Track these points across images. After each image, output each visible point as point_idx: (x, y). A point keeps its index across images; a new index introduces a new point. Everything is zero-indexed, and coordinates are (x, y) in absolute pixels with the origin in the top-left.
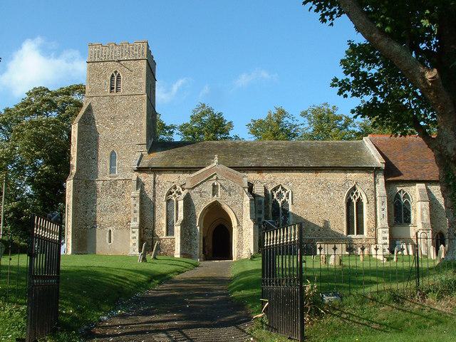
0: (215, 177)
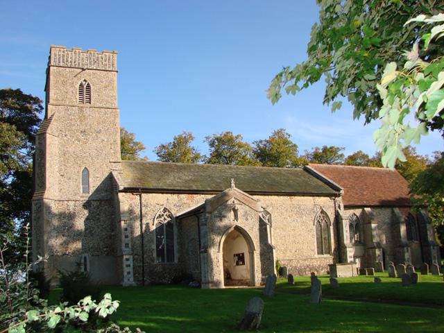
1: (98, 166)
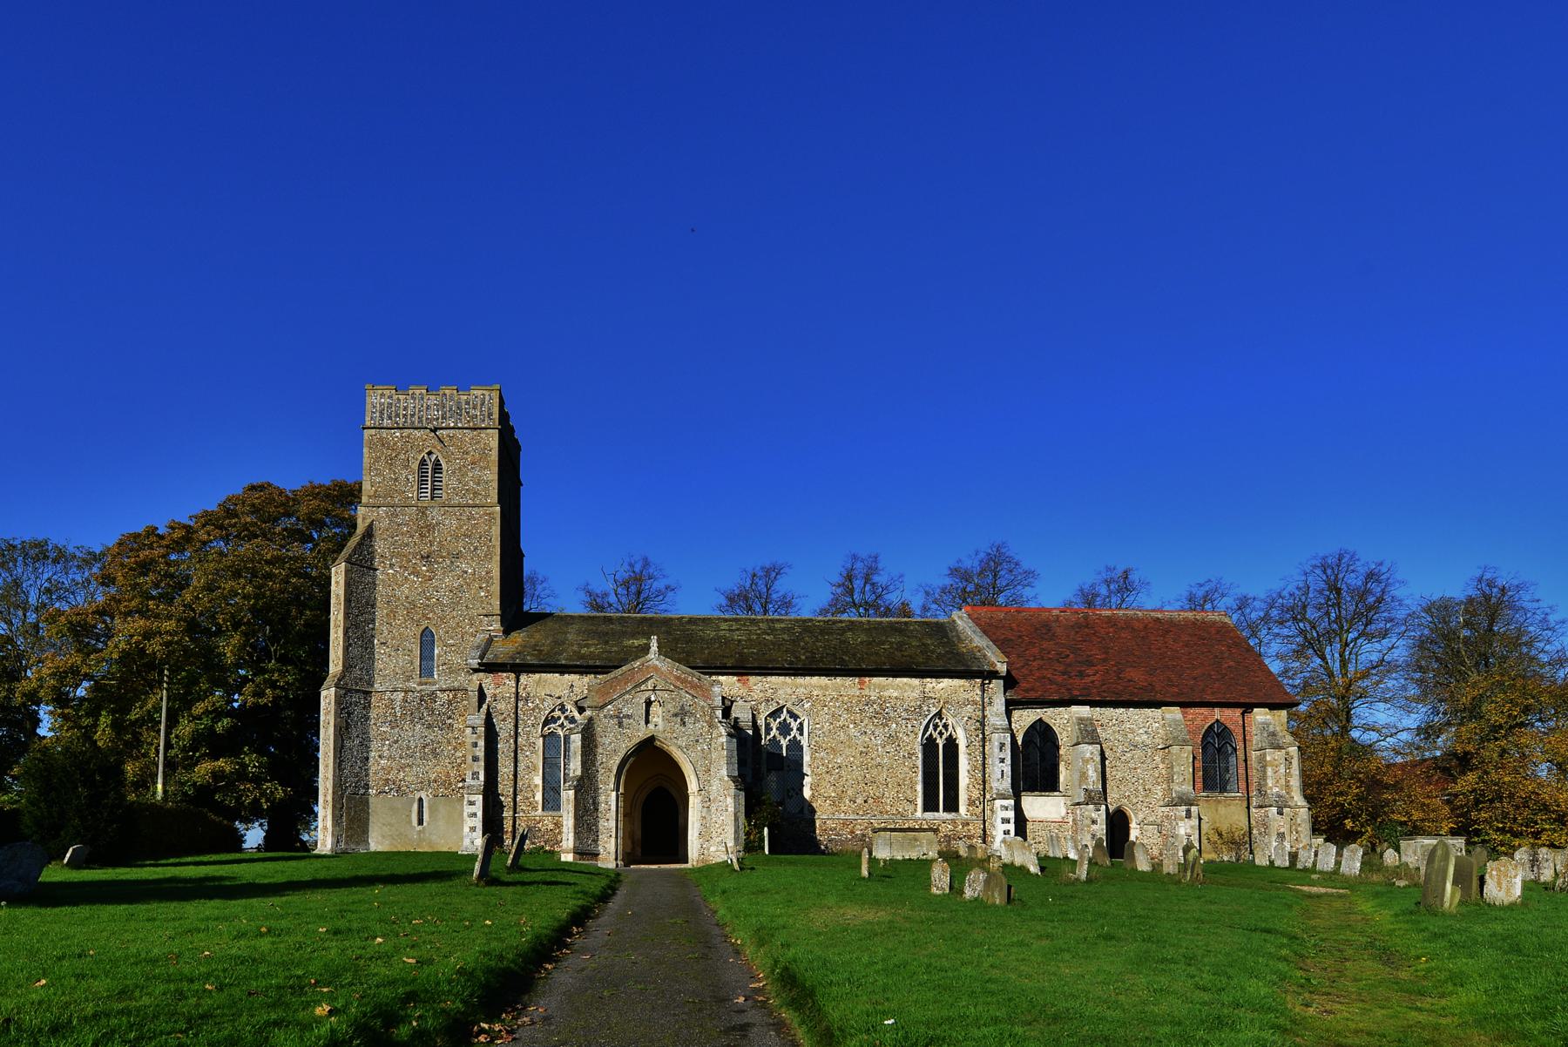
0: (650, 685)
1: (452, 623)
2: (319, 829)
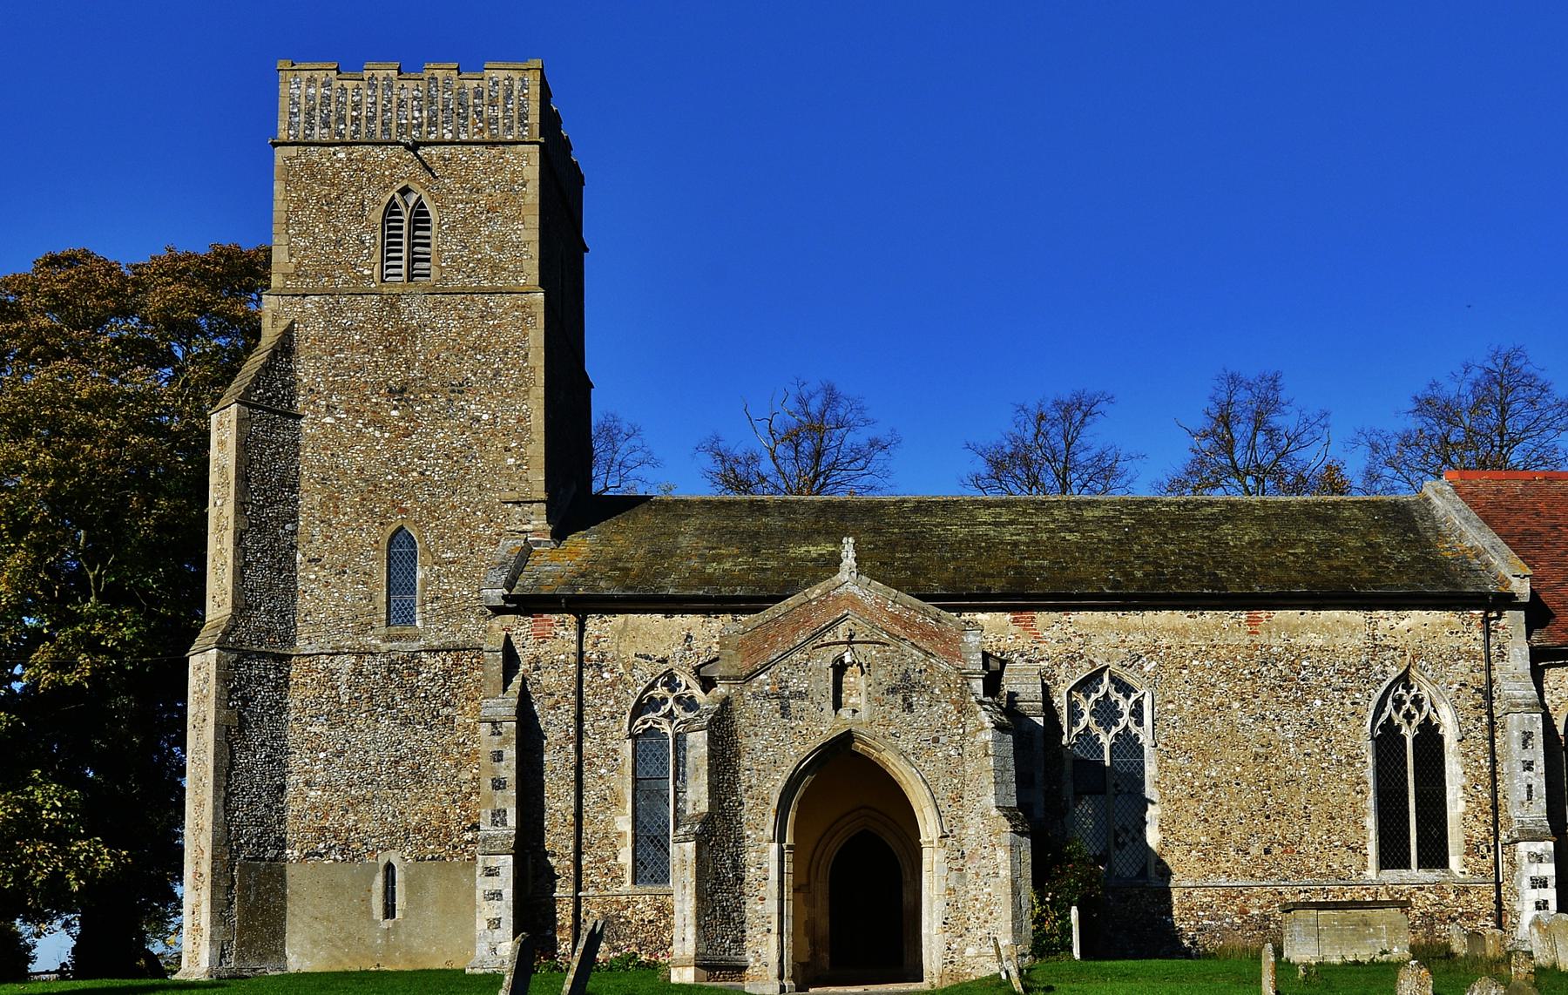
0: (842, 632)
1: (451, 519)
2: (184, 931)
